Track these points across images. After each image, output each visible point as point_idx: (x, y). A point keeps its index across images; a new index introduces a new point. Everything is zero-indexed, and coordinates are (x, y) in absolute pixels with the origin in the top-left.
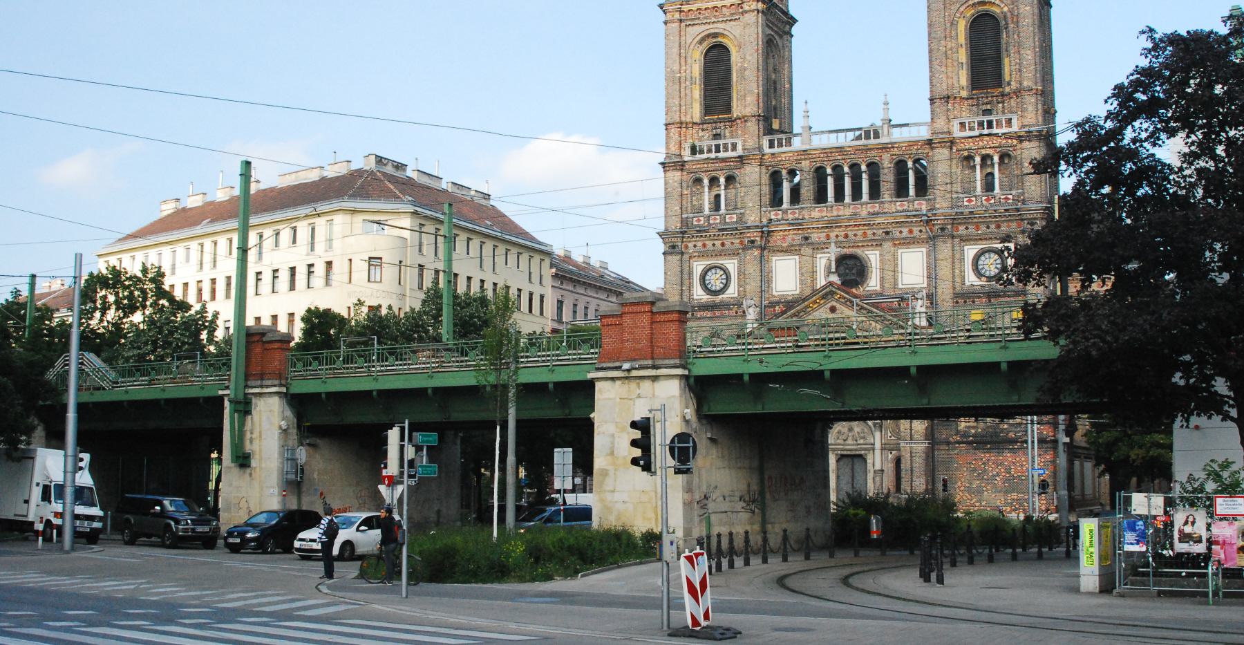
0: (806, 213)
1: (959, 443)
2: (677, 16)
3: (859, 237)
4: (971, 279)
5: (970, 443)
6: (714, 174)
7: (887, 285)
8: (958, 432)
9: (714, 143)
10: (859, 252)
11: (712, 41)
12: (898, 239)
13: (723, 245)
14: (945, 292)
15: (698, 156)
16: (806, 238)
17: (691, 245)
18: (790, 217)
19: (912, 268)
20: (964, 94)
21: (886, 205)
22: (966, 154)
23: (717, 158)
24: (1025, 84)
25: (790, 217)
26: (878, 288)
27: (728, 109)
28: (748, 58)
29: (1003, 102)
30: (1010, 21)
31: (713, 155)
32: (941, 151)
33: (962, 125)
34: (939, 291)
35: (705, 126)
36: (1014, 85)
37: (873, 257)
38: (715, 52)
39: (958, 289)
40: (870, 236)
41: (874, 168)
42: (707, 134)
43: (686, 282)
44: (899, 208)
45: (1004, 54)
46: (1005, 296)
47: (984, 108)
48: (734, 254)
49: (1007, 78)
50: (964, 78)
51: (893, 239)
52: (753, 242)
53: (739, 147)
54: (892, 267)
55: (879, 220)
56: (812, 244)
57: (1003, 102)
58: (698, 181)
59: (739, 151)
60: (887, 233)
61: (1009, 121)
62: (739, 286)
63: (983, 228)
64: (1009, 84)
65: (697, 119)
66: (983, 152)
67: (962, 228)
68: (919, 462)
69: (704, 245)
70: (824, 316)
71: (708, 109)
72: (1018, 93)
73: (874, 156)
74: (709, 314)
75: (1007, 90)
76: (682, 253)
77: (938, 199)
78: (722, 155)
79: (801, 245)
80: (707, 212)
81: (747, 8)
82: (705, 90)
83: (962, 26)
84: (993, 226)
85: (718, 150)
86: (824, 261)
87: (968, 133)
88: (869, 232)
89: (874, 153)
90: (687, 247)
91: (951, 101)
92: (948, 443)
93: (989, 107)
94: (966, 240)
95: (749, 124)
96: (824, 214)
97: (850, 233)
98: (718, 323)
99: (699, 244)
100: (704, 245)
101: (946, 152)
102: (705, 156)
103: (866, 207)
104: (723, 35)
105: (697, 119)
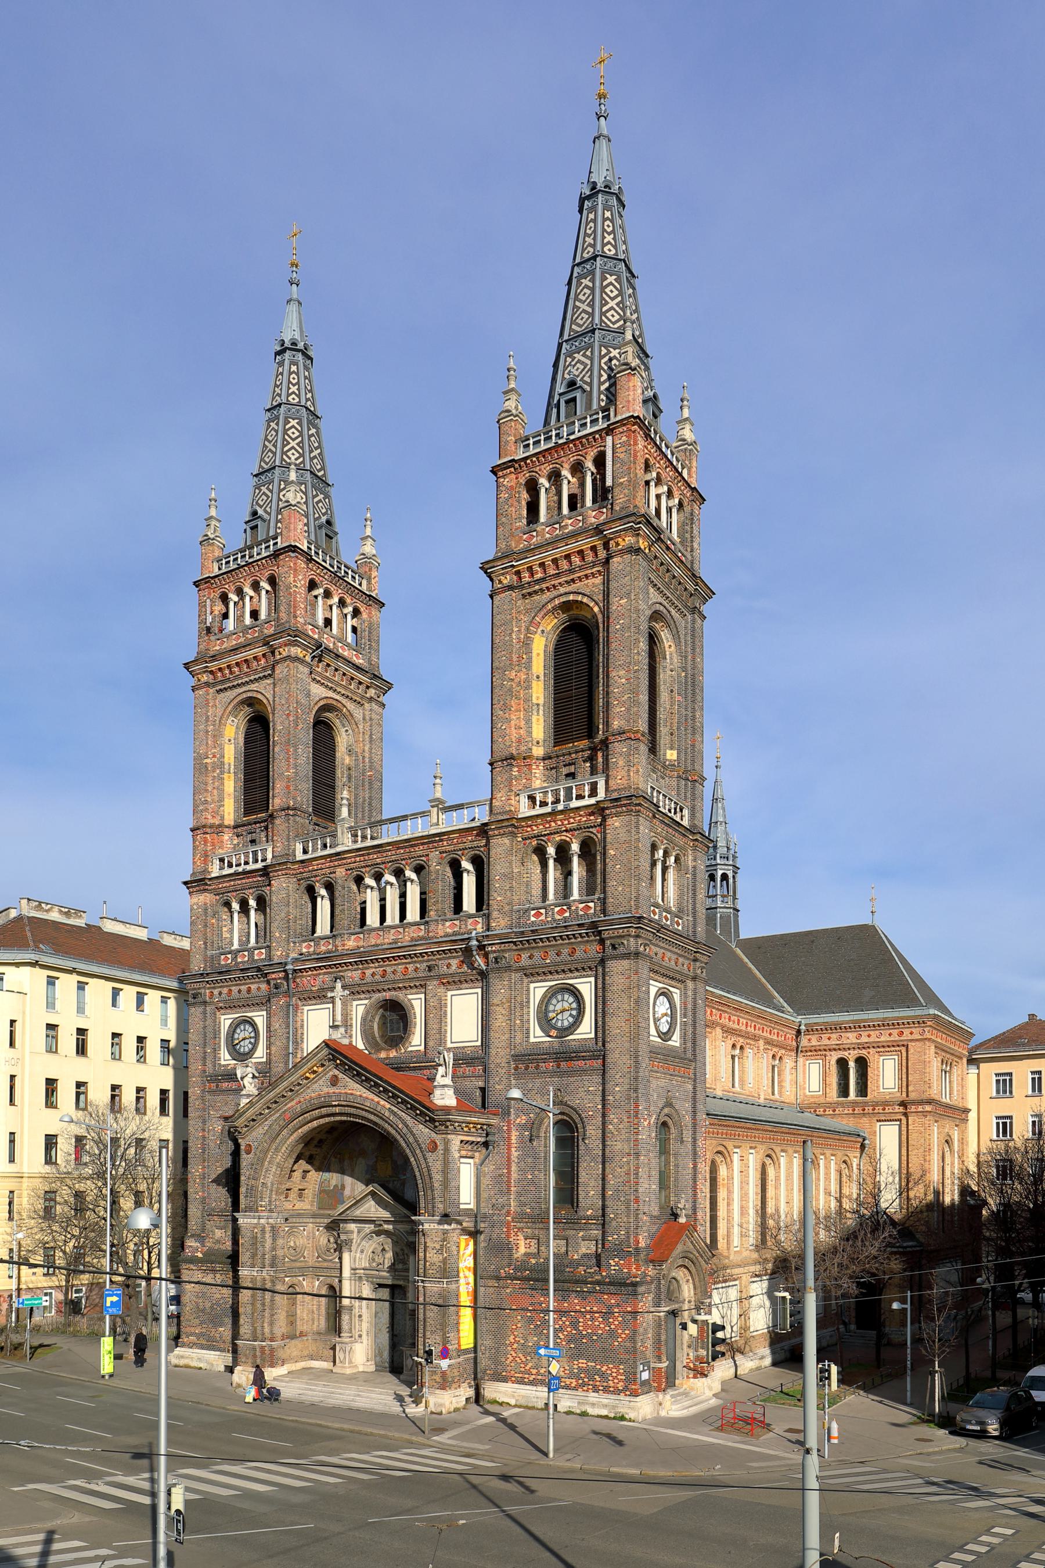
3: (399, 976)
4: (537, 1035)
7: (431, 1044)
10: (399, 996)
12: (445, 976)
13: (249, 990)
14: (500, 1054)
19: (463, 1016)
20: (538, 751)
22: (535, 843)
26: (422, 1048)
33: (532, 798)
34: (493, 1052)
37: (416, 1002)
39: (520, 1050)
40: (413, 975)
44: (448, 930)
46: (578, 1058)
51: (439, 977)
52: (277, 987)
53: (269, 856)
54: (437, 1014)
55: (420, 950)
58: (228, 904)
63: (552, 953)
67: (525, 955)
70: (326, 1090)
83: (541, 646)
84: (565, 951)
86: (359, 1009)
88: (411, 967)
89: (420, 850)
92: (498, 1278)
93: (572, 769)
94: (533, 974)
96: (361, 943)
97: (389, 970)
99: (225, 991)
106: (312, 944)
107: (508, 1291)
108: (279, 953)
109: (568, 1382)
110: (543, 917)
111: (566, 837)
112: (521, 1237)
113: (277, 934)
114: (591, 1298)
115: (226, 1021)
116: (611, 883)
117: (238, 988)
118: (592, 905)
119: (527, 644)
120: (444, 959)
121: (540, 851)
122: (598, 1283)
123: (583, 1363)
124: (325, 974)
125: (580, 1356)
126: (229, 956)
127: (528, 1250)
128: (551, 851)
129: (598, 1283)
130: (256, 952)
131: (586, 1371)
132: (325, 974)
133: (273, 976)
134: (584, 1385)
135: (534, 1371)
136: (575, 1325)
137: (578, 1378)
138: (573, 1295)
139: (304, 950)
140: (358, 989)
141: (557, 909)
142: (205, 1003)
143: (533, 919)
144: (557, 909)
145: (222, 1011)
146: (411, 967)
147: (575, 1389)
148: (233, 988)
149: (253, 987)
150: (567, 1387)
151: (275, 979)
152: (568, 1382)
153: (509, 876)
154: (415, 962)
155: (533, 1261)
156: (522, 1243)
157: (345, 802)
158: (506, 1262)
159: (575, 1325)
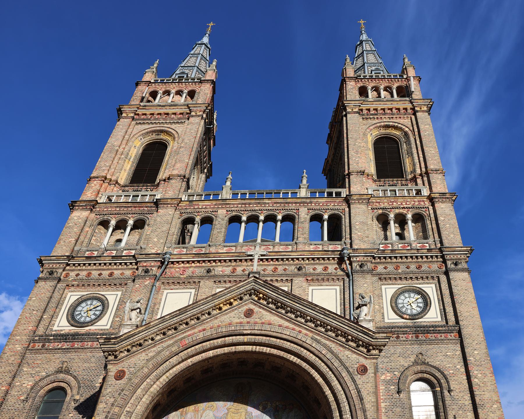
13: (111, 275)
16: (209, 271)
17: (73, 274)
43: (50, 311)
48: (121, 284)
52: (147, 271)
56: (215, 276)
62: (116, 316)
69: (89, 274)
74: (66, 345)
76: (59, 280)
79: (202, 277)
88: (280, 269)
90: (67, 275)
98: (72, 355)
100: (89, 274)
106: (185, 250)
115: (72, 297)
117: (99, 272)
119: (365, 135)
120: (312, 264)
124: (196, 267)
132: (196, 267)
133: (145, 264)
140: (227, 279)
142: (59, 280)
145: (72, 289)
148: (93, 272)
149: (116, 272)
151: (146, 266)
154: (286, 264)
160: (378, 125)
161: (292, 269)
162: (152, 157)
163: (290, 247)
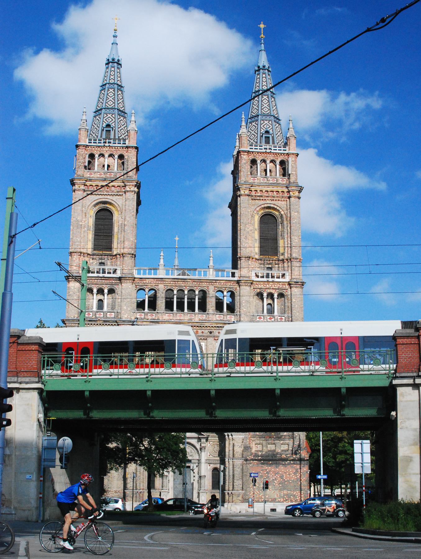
0: (159, 315)
1: (253, 460)
2: (82, 187)
5: (260, 460)
6: (100, 286)
8: (252, 454)
9: (102, 267)
11: (102, 206)
15: (90, 275)
18: (150, 317)
21: (211, 316)
22: (259, 291)
23: (104, 277)
24: (294, 255)
25: (150, 317)
27: (110, 249)
28: (127, 219)
29: (278, 264)
30: (285, 219)
31: (101, 275)
32: (245, 287)
35: (95, 257)
36: (286, 257)
38: (102, 213)
41: (204, 294)
42: (95, 262)
44: (218, 318)
45: (279, 237)
47: (268, 266)
49: (281, 250)
50: (257, 250)
51: (214, 336)
55: (207, 325)
57: (278, 264)
59: (118, 274)
60: (211, 333)
61: (283, 275)
64: (283, 254)
65: (90, 251)
66: (269, 291)
68: (238, 471)
71: (96, 247)
72: (290, 260)
73: (204, 286)
75: (281, 258)
77: (242, 316)
78: (106, 275)
80: (95, 309)
81: (128, 189)
82: (95, 235)
83: (257, 218)
85: (104, 272)
87: (260, 279)
88: (200, 331)
89: (204, 284)
91: (251, 259)
93: (270, 266)
95: (126, 258)
96: (171, 318)
101: (248, 288)
102: (96, 275)
103: (197, 316)
104: (110, 204)
105: (90, 251)
106: (143, 314)
107: (251, 465)
108: (126, 316)
109: (279, 500)
110: (262, 319)
111: (273, 291)
112: (254, 443)
113: (125, 308)
114: (289, 466)
116: (293, 311)
118: (283, 318)
119: (253, 216)
121: (260, 295)
122: (292, 460)
123: (285, 492)
125: (284, 489)
126: (91, 313)
127: (257, 449)
128: (265, 295)
129: (292, 460)
130: (108, 314)
131: (287, 495)
134: (286, 500)
135: (263, 497)
136: (282, 477)
137: (283, 498)
138: (281, 465)
139: (138, 317)
141: (268, 317)
143: (258, 319)
144: (268, 317)
146: (200, 331)
147: (283, 502)
150: (279, 502)
152: (279, 500)
153: (247, 302)
155: (260, 453)
156: (254, 446)
157: (162, 257)
158: (249, 454)
159: (282, 477)
160: (263, 206)
161: (206, 332)
162: (104, 218)
163: (205, 315)
